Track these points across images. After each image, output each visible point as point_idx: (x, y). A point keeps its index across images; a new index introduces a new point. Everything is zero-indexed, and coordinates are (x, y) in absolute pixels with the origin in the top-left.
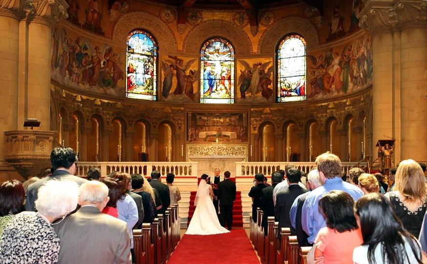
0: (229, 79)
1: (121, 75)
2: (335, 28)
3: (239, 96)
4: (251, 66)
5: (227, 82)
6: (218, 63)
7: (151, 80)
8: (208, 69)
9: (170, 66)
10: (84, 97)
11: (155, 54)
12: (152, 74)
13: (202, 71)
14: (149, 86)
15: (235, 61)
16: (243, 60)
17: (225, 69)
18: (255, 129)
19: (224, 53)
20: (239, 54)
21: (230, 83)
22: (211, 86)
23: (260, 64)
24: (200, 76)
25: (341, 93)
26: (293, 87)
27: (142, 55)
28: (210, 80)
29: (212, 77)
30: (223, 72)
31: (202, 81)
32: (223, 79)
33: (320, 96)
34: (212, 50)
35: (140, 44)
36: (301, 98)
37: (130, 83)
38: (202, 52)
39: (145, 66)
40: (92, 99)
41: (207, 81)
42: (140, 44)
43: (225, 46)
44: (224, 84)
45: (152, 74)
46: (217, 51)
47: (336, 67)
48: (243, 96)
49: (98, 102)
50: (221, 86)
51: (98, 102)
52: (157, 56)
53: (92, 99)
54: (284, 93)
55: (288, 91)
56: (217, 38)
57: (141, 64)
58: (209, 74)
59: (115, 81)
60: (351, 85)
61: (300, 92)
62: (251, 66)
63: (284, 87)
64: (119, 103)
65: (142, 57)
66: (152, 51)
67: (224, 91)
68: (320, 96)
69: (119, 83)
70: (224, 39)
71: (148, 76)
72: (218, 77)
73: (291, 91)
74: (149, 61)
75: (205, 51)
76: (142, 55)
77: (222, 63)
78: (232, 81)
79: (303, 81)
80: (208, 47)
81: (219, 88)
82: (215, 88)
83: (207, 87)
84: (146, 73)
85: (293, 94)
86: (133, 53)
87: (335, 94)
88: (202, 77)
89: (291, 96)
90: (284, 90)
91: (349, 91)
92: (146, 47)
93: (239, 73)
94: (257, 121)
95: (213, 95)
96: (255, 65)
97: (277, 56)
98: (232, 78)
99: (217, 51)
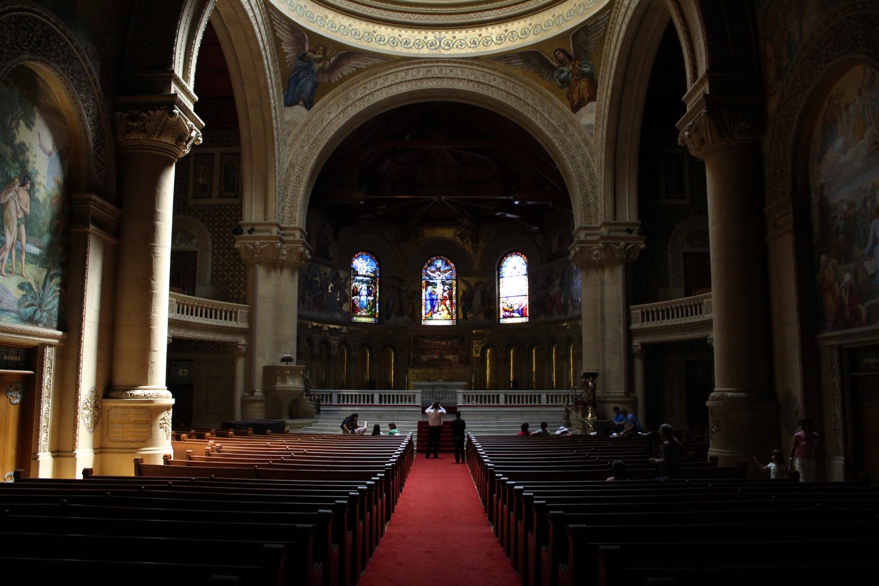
0: (451, 298)
1: (346, 299)
2: (555, 247)
3: (461, 317)
4: (473, 285)
5: (448, 302)
6: (439, 282)
7: (374, 301)
8: (430, 288)
9: (393, 287)
10: (315, 324)
11: (378, 274)
12: (375, 296)
13: (424, 290)
14: (371, 308)
15: (456, 280)
16: (466, 279)
17: (446, 288)
18: (477, 352)
19: (445, 272)
20: (461, 273)
21: (452, 304)
22: (433, 307)
23: (482, 283)
24: (421, 296)
25: (562, 316)
26: (515, 308)
27: (365, 276)
28: (432, 300)
29: (434, 297)
30: (444, 291)
31: (424, 301)
32: (445, 299)
33: (542, 318)
34: (433, 269)
35: (363, 265)
36: (524, 320)
37: (354, 305)
38: (424, 271)
39: (368, 287)
40: (321, 325)
41: (428, 302)
42: (363, 265)
43: (447, 264)
44: (445, 305)
45: (375, 296)
46: (439, 269)
47: (557, 289)
48: (465, 317)
49: (326, 328)
50: (443, 306)
51: (326, 328)
52: (380, 277)
53: (321, 325)
54: (507, 314)
55: (510, 312)
56: (439, 256)
57: (365, 286)
58: (431, 294)
59: (341, 304)
60: (571, 308)
61: (522, 314)
62: (473, 285)
63: (506, 308)
64: (345, 328)
65: (366, 279)
66: (375, 272)
67: (446, 312)
68: (542, 318)
69: (346, 307)
70: (445, 256)
71: (371, 298)
72: (440, 297)
73: (513, 311)
74: (372, 283)
75: (426, 269)
76: (365, 276)
77: (443, 283)
78: (454, 301)
79: (525, 302)
80: (430, 265)
81: (440, 309)
82: (436, 309)
83: (429, 307)
84: (369, 295)
85: (515, 314)
86: (358, 275)
87: (557, 316)
88: (423, 298)
89: (513, 317)
90: (506, 311)
91: (569, 315)
92: (369, 268)
93: (460, 294)
94: (479, 344)
95: (435, 316)
96: (477, 284)
97: (499, 274)
98: (454, 297)
99: (439, 269)
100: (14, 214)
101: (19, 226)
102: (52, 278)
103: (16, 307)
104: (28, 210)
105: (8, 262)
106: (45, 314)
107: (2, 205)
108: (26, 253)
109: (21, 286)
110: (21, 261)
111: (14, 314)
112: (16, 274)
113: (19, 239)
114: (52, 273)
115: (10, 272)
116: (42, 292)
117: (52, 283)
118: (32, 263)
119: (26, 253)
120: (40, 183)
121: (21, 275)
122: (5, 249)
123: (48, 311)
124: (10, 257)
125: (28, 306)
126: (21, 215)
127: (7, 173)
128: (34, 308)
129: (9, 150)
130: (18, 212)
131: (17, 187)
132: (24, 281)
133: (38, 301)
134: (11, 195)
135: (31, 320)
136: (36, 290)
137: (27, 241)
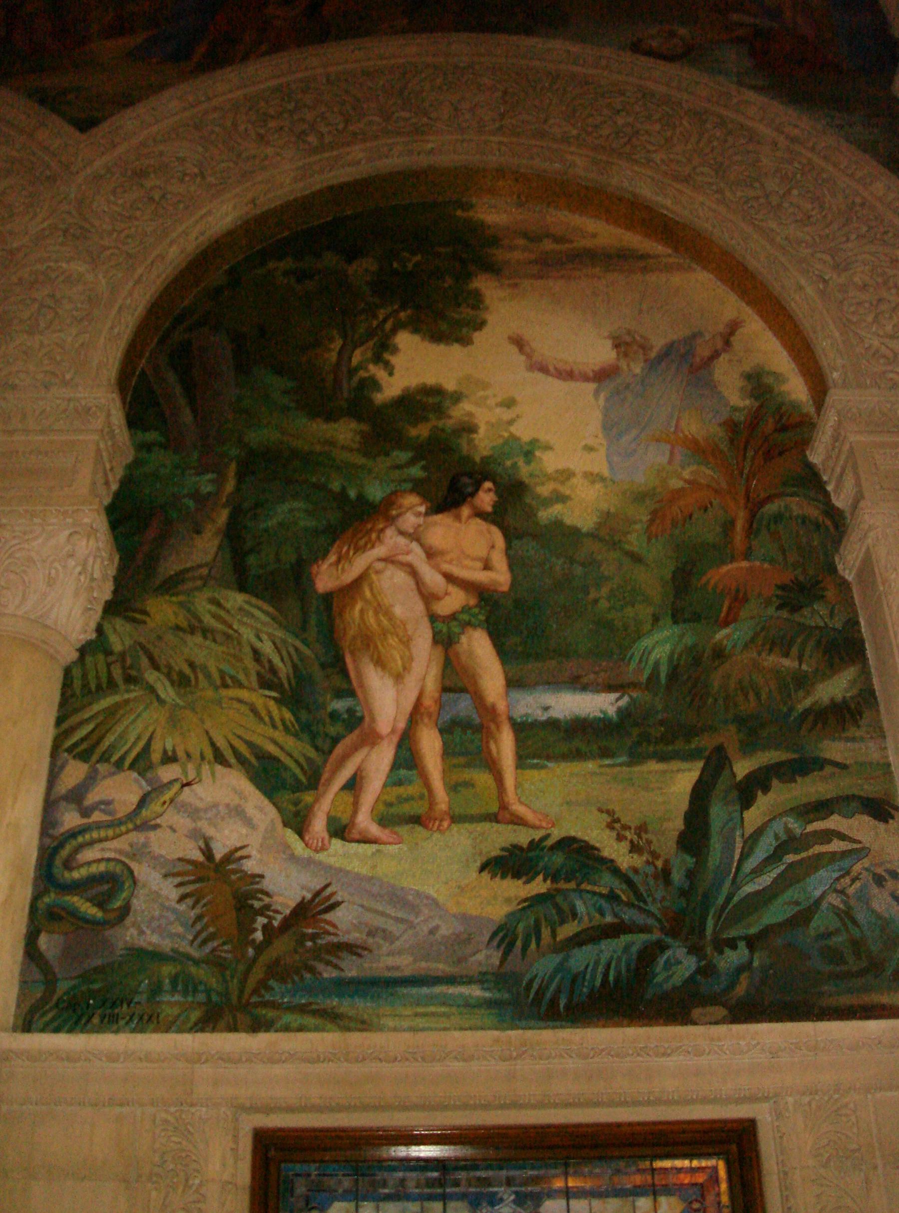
100: (406, 607)
101: (445, 640)
102: (747, 792)
103: (486, 958)
104: (500, 576)
105: (394, 781)
106: (732, 958)
107: (328, 598)
108: (521, 728)
109: (510, 864)
110: (493, 766)
111: (476, 992)
112: (456, 819)
113: (456, 679)
114: (742, 768)
115: (416, 820)
116: (680, 865)
117: (753, 816)
118: (578, 755)
119: (521, 728)
120: (566, 475)
121: (501, 815)
122: (372, 739)
123: (752, 943)
124: (407, 758)
125: (578, 941)
126: (454, 600)
127: (342, 496)
128: (640, 939)
129: (345, 432)
130: (428, 597)
131: (410, 521)
132: (523, 837)
133: (659, 900)
134: (380, 551)
135: (625, 999)
136: (623, 857)
137: (513, 683)
